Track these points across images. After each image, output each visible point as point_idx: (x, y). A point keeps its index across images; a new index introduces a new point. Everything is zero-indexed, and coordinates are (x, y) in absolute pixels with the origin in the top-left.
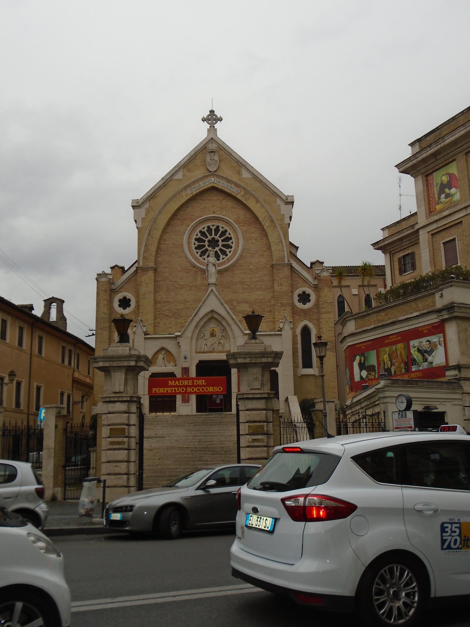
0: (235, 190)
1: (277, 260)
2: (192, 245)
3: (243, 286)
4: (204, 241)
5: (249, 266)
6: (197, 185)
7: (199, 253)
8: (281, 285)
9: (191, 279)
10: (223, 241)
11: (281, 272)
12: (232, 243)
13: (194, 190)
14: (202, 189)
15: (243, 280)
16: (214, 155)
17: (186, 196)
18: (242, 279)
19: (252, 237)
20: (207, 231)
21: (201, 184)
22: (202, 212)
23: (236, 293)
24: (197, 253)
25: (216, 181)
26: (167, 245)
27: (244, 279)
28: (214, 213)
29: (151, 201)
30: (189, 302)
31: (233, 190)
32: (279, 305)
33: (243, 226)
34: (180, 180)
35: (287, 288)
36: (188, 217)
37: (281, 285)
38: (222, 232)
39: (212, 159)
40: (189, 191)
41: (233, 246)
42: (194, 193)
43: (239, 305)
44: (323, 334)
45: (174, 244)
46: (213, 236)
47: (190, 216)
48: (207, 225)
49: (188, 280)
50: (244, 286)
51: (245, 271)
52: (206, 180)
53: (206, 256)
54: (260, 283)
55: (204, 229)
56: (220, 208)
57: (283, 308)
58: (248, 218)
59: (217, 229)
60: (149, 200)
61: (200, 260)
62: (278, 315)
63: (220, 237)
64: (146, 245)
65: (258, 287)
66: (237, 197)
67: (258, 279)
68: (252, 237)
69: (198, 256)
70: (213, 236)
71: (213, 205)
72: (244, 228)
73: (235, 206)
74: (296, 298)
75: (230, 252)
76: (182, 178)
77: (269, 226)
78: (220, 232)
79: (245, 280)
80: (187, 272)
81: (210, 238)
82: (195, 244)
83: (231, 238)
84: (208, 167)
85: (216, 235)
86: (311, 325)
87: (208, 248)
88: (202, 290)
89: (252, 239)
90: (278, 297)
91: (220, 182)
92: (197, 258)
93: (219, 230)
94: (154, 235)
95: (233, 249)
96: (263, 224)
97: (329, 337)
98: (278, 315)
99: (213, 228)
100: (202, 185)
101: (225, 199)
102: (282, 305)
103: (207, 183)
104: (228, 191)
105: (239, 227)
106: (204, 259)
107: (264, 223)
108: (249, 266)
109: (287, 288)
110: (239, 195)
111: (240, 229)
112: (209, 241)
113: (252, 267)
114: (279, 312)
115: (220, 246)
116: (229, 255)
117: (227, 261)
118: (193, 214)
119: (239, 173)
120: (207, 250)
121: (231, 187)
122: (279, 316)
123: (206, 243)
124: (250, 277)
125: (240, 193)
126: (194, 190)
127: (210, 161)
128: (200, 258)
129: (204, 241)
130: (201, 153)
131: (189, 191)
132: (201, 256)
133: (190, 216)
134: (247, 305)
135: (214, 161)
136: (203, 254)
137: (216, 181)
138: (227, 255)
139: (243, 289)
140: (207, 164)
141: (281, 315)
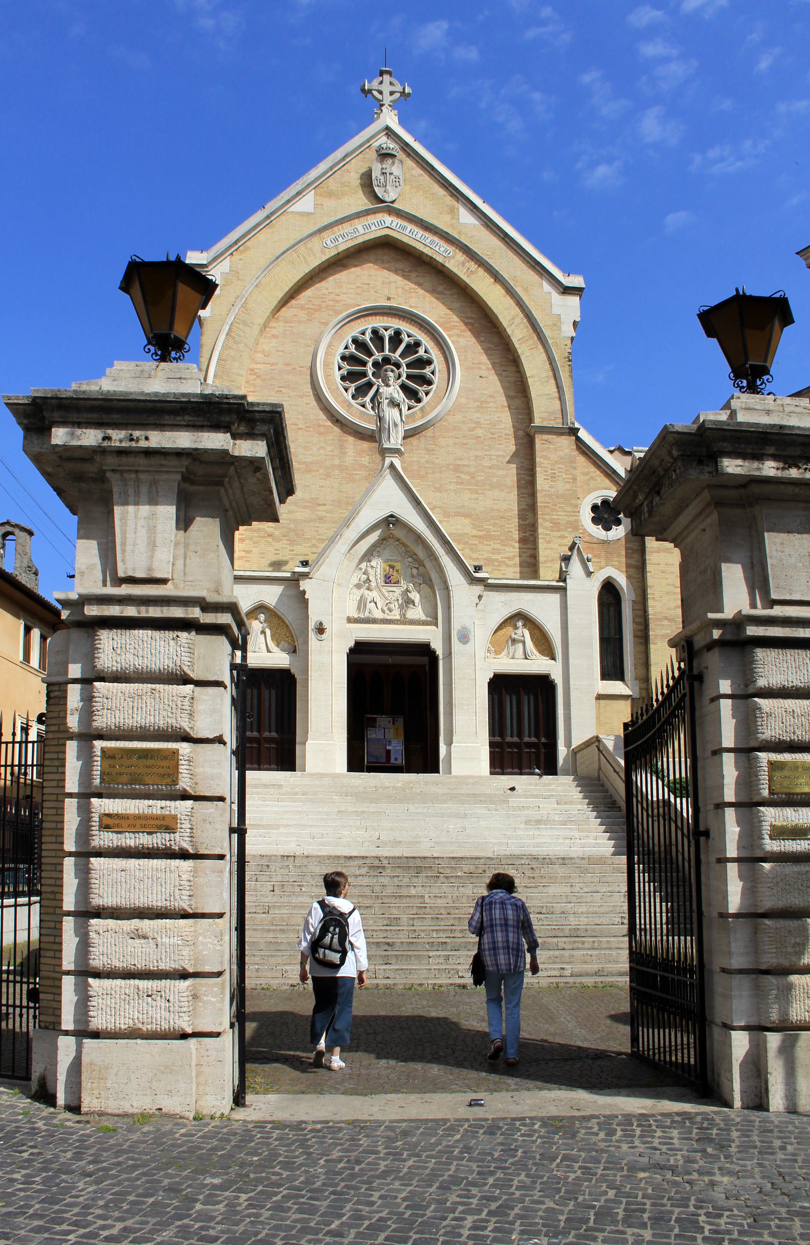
0: (442, 249)
1: (543, 419)
2: (333, 369)
3: (459, 477)
4: (364, 364)
5: (472, 430)
6: (346, 228)
7: (352, 390)
8: (553, 477)
9: (329, 449)
10: (409, 366)
11: (552, 446)
12: (433, 373)
13: (340, 240)
14: (360, 240)
15: (459, 462)
16: (393, 163)
17: (323, 253)
18: (455, 459)
19: (480, 363)
20: (371, 339)
21: (360, 227)
22: (358, 294)
23: (441, 492)
24: (346, 390)
25: (394, 224)
26: (272, 365)
27: (461, 459)
28: (389, 299)
29: (237, 256)
30: (325, 505)
31: (437, 249)
32: (548, 524)
33: (458, 336)
34: (309, 214)
35: (568, 486)
36: (324, 305)
37: (553, 477)
38: (408, 346)
39: (388, 171)
40: (329, 243)
41: (436, 379)
42: (342, 248)
43: (448, 522)
44: (654, 599)
45: (288, 365)
46: (387, 352)
47: (331, 303)
48: (371, 326)
49: (322, 451)
50: (462, 476)
51: (465, 441)
52: (372, 219)
53: (368, 399)
54: (501, 472)
55: (363, 334)
56: (403, 289)
57: (559, 534)
58: (472, 318)
59: (396, 338)
60: (232, 254)
61: (352, 406)
62: (545, 549)
63: (402, 355)
64: (219, 359)
65: (495, 480)
66: (447, 265)
67: (494, 462)
68: (480, 363)
69: (348, 396)
70: (387, 352)
71: (387, 281)
72: (461, 339)
73: (440, 288)
74: (587, 515)
75: (427, 394)
76: (312, 211)
77: (523, 338)
78: (402, 347)
79: (466, 463)
80: (320, 433)
81: (378, 356)
82: (340, 369)
83: (429, 362)
84: (376, 189)
85: (393, 349)
86: (621, 580)
87: (373, 379)
88: (357, 477)
89: (480, 368)
90: (545, 507)
91: (404, 228)
92: (346, 401)
93: (401, 341)
94: (240, 336)
95: (434, 387)
96: (509, 331)
97: (668, 609)
98: (545, 549)
99: (387, 335)
100: (362, 231)
101: (416, 271)
102: (556, 525)
103: (373, 228)
104: (426, 251)
105: (449, 336)
106: (363, 406)
107: (513, 331)
108: (472, 430)
109: (568, 486)
110: (452, 261)
111: (453, 342)
112: (376, 364)
113: (479, 432)
114: (549, 542)
115: (404, 377)
116: (426, 399)
117: (419, 414)
118: (338, 298)
119: (452, 211)
120: (370, 385)
121: (432, 242)
122: (549, 552)
123: (370, 369)
124: (477, 456)
125: (453, 257)
126: (340, 240)
127: (382, 178)
128: (353, 402)
129: (364, 364)
130: (361, 156)
131: (329, 243)
132: (353, 397)
133: (331, 303)
134: (467, 521)
135: (392, 177)
136: (361, 391)
137: (394, 224)
138: (419, 401)
139: (457, 483)
140: (375, 183)
141: (552, 549)
